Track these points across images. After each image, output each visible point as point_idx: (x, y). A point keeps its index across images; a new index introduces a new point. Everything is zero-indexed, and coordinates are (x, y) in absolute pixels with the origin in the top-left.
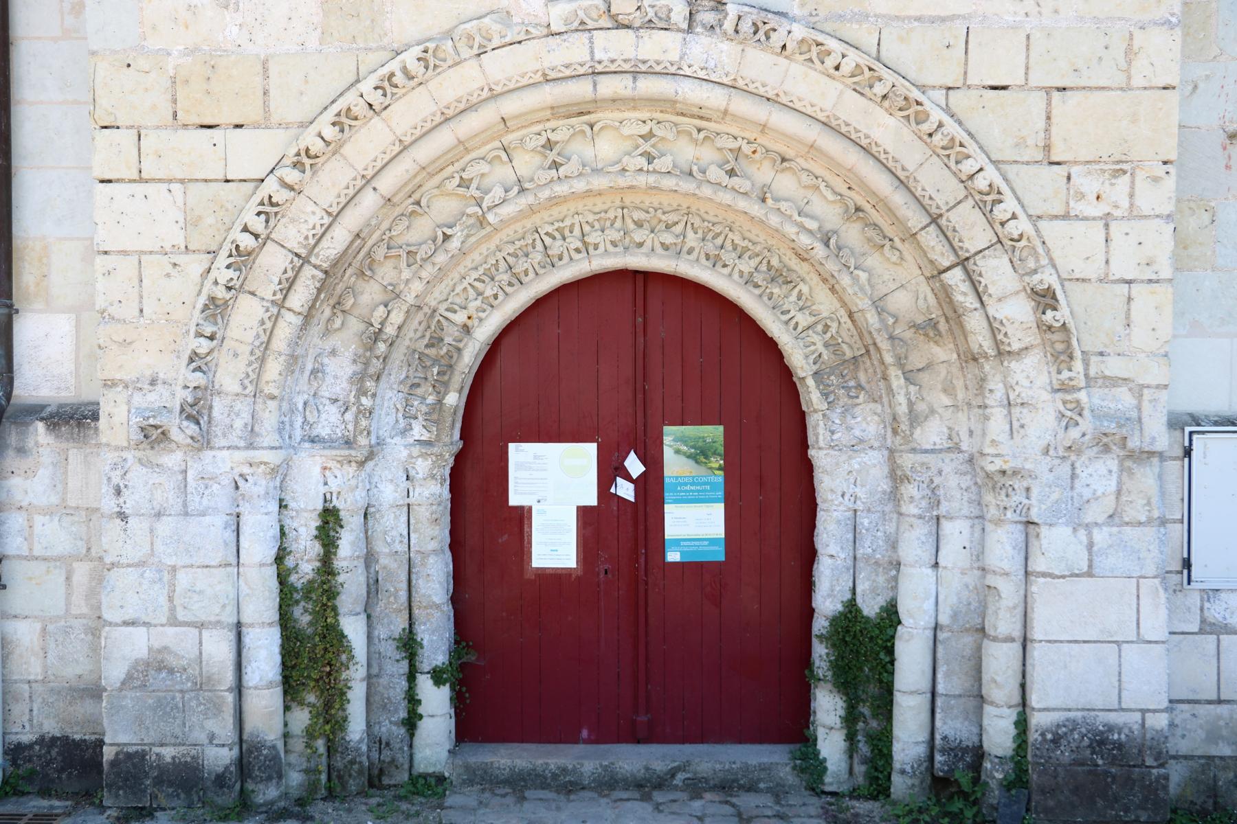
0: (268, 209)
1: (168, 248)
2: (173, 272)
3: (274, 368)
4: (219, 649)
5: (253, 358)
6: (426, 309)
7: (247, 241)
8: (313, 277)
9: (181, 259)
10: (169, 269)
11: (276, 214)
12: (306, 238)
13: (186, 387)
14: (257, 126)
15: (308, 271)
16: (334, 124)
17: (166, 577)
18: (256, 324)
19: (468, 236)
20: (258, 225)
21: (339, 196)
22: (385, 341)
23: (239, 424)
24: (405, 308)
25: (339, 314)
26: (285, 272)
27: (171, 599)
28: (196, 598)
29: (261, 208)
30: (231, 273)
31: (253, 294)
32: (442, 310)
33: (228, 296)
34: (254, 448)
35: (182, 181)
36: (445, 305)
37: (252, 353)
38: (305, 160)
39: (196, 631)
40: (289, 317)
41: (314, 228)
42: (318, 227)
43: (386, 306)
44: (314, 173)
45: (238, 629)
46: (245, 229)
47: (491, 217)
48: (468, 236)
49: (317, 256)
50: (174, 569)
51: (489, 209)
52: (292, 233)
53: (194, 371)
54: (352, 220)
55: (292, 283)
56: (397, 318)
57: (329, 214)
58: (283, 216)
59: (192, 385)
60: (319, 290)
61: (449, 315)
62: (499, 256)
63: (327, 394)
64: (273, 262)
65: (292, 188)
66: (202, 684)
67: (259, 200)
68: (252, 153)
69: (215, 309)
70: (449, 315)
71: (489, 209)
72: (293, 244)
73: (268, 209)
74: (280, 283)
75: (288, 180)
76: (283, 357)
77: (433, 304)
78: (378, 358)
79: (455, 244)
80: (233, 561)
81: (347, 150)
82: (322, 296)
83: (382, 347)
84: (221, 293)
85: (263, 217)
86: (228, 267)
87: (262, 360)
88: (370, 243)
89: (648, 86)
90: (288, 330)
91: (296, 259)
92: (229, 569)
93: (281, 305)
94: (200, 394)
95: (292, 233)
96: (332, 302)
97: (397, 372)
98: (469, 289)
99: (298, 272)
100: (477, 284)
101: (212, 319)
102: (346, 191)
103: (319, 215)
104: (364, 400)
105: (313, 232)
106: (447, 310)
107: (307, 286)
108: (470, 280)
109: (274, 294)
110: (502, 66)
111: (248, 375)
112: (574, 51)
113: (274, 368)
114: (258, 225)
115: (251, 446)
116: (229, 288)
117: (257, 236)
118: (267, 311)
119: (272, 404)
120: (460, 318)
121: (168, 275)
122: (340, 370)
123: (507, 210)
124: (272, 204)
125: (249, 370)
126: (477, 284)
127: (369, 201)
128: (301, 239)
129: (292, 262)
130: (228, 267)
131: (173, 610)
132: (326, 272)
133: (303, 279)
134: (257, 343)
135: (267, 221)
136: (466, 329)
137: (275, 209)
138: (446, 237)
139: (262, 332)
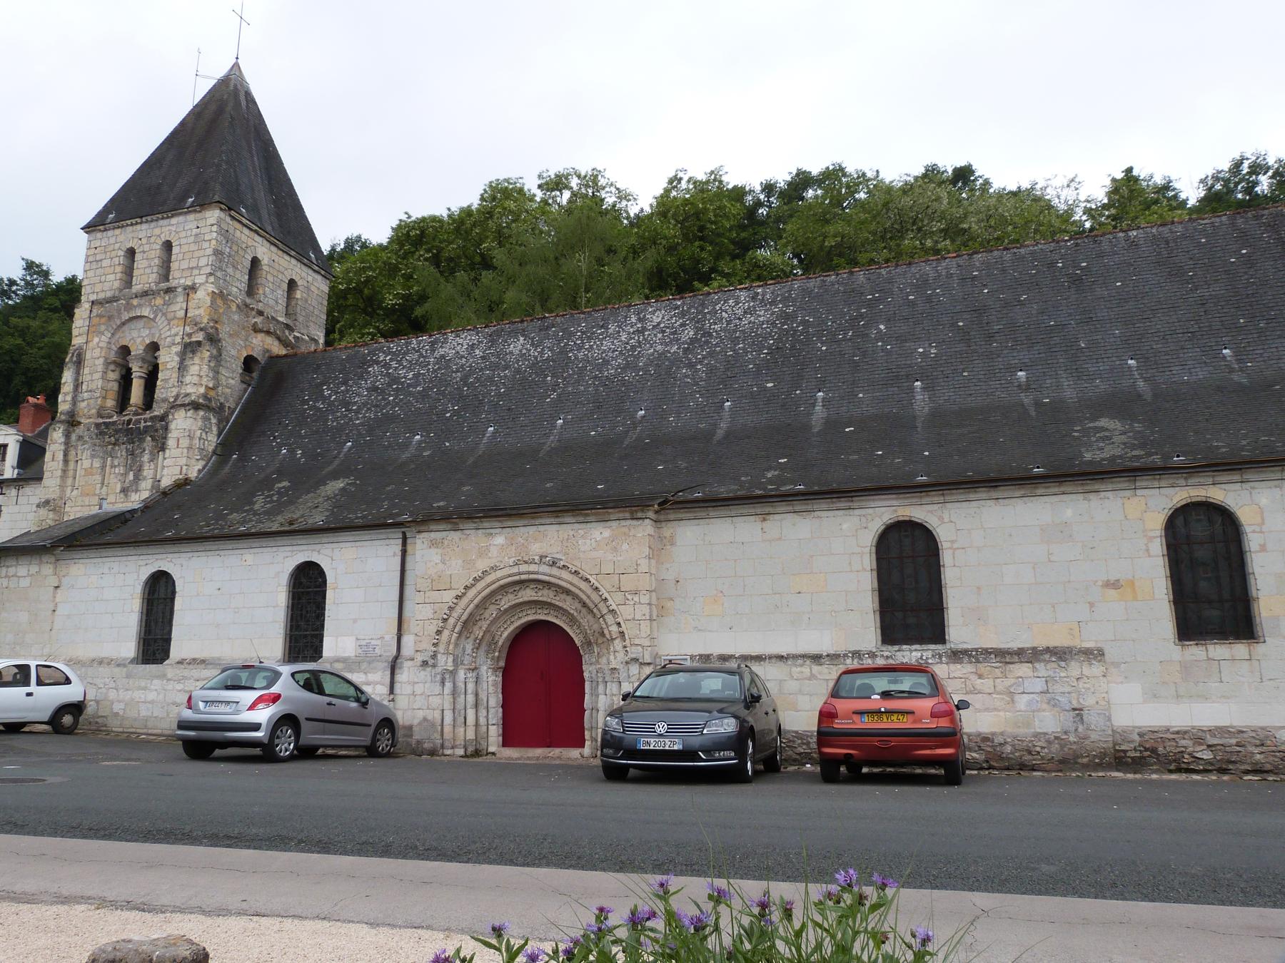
3: (451, 647)
4: (437, 715)
38: (458, 597)
52: (455, 615)
54: (468, 611)
64: (451, 621)
66: (433, 725)
68: (448, 597)
69: (439, 632)
89: (532, 576)
95: (455, 615)
97: (484, 647)
110: (499, 574)
112: (515, 570)
113: (451, 647)
122: (469, 648)
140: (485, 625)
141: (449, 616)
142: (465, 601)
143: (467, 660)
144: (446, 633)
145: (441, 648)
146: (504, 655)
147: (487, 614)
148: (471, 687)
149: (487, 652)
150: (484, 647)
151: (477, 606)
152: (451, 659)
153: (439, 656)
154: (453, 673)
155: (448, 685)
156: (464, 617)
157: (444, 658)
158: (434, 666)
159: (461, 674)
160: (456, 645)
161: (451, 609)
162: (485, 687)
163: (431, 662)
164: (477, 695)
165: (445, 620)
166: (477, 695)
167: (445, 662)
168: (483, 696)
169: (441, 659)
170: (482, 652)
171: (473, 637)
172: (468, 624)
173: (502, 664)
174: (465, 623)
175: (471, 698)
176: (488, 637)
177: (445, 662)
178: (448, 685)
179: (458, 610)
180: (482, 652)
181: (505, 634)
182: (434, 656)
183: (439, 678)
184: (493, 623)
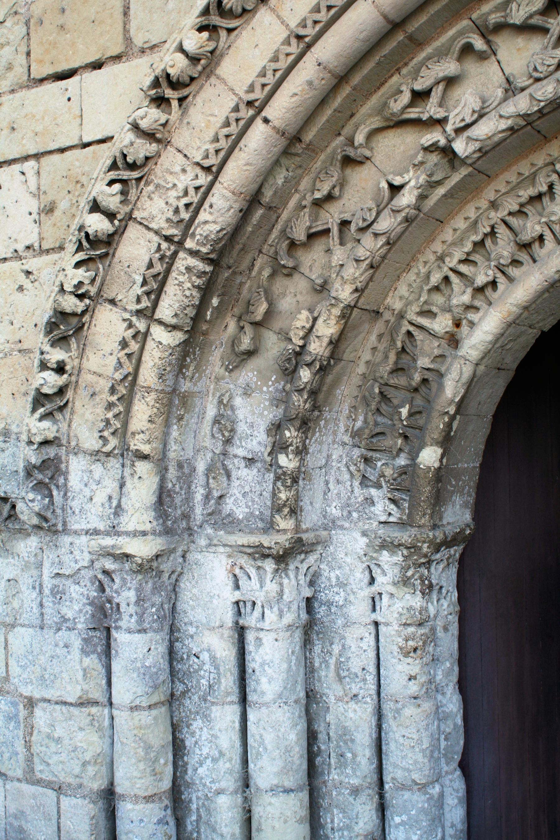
0: (125, 174)
1: (20, 247)
2: (27, 283)
3: (142, 412)
5: (114, 398)
6: (387, 315)
7: (98, 224)
8: (189, 269)
9: (33, 263)
10: (22, 279)
11: (139, 180)
12: (177, 211)
13: (30, 443)
14: (118, 58)
15: (184, 261)
16: (201, 29)
17: (23, 713)
18: (116, 346)
19: (432, 185)
20: (111, 197)
21: (216, 140)
22: (309, 365)
23: (100, 497)
24: (336, 311)
25: (248, 329)
26: (150, 265)
27: (28, 745)
28: (53, 747)
29: (113, 175)
30: (82, 274)
31: (112, 302)
32: (411, 315)
33: (80, 306)
34: (118, 534)
35: (37, 156)
36: (415, 308)
37: (113, 390)
38: (169, 91)
39: (52, 794)
40: (158, 332)
41: (186, 193)
42: (192, 192)
43: (311, 310)
44: (184, 113)
45: (109, 797)
46: (95, 207)
47: (460, 147)
48: (432, 185)
49: (193, 235)
50: (31, 703)
51: (459, 131)
52: (156, 208)
53: (41, 419)
55: (162, 279)
56: (327, 329)
57: (208, 169)
58: (147, 184)
59: (38, 439)
60: (206, 292)
61: (424, 321)
62: (495, 216)
63: (241, 452)
64: (136, 250)
65: (149, 136)
67: (109, 162)
70: (424, 321)
71: (459, 131)
72: (159, 223)
73: (125, 174)
74: (145, 283)
75: (144, 124)
76: (153, 395)
77: (398, 306)
78: (300, 391)
79: (407, 198)
80: (98, 694)
81: (227, 68)
82: (215, 302)
83: (305, 375)
84: (71, 304)
85: (117, 187)
86: (78, 265)
87: (127, 401)
88: (285, 216)
90: (157, 354)
91: (164, 245)
92: (94, 710)
93: (148, 314)
94: (51, 452)
95: (156, 208)
96: (237, 311)
97: (342, 419)
98: (454, 278)
99: (170, 265)
100: (463, 268)
101: (61, 341)
102: (226, 131)
103: (190, 175)
104: (283, 460)
105: (185, 200)
106: (422, 313)
107: (180, 284)
108: (452, 262)
109: (139, 301)
111: (108, 422)
113: (142, 412)
114: (111, 197)
115: (114, 531)
116: (81, 297)
117: (111, 216)
118: (130, 326)
119: (142, 467)
120: (441, 324)
121: (21, 288)
122: (254, 417)
123: (485, 129)
124: (133, 167)
125: (110, 415)
126: (463, 268)
127: (258, 140)
128: (170, 214)
129: (159, 249)
130: (78, 265)
131: (29, 760)
132: (211, 261)
133: (174, 274)
134: (118, 376)
135: (124, 193)
136: (453, 341)
137: (136, 174)
138: (395, 189)
139: (124, 360)
140: (343, 267)
141: (121, 221)
142: (211, 108)
143: (247, 492)
144: (108, 327)
145: (85, 423)
146: (470, 462)
147: (360, 193)
148: (273, 656)
149: (370, 443)
150: (342, 419)
151: (292, 143)
152: (142, 489)
153: (77, 469)
154: (162, 576)
155: (136, 648)
156: (216, 217)
157: (106, 476)
158: (49, 526)
159: (212, 583)
160: (174, 404)
161: (129, 172)
162: (360, 656)
163: (29, 505)
164: (311, 703)
165: (98, 249)
166: (311, 703)
167: (107, 501)
168: (350, 717)
169: (88, 486)
170: (334, 449)
171: (273, 347)
172: (232, 270)
173: (458, 515)
174: (223, 256)
175: (277, 731)
176: (368, 351)
177: (107, 501)
178: (136, 648)
179: (175, 175)
180: (334, 449)
181: (487, 326)
182: (46, 473)
183: (77, 602)
184: (398, 251)
